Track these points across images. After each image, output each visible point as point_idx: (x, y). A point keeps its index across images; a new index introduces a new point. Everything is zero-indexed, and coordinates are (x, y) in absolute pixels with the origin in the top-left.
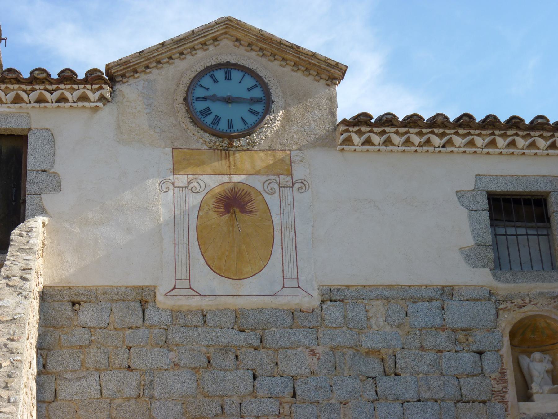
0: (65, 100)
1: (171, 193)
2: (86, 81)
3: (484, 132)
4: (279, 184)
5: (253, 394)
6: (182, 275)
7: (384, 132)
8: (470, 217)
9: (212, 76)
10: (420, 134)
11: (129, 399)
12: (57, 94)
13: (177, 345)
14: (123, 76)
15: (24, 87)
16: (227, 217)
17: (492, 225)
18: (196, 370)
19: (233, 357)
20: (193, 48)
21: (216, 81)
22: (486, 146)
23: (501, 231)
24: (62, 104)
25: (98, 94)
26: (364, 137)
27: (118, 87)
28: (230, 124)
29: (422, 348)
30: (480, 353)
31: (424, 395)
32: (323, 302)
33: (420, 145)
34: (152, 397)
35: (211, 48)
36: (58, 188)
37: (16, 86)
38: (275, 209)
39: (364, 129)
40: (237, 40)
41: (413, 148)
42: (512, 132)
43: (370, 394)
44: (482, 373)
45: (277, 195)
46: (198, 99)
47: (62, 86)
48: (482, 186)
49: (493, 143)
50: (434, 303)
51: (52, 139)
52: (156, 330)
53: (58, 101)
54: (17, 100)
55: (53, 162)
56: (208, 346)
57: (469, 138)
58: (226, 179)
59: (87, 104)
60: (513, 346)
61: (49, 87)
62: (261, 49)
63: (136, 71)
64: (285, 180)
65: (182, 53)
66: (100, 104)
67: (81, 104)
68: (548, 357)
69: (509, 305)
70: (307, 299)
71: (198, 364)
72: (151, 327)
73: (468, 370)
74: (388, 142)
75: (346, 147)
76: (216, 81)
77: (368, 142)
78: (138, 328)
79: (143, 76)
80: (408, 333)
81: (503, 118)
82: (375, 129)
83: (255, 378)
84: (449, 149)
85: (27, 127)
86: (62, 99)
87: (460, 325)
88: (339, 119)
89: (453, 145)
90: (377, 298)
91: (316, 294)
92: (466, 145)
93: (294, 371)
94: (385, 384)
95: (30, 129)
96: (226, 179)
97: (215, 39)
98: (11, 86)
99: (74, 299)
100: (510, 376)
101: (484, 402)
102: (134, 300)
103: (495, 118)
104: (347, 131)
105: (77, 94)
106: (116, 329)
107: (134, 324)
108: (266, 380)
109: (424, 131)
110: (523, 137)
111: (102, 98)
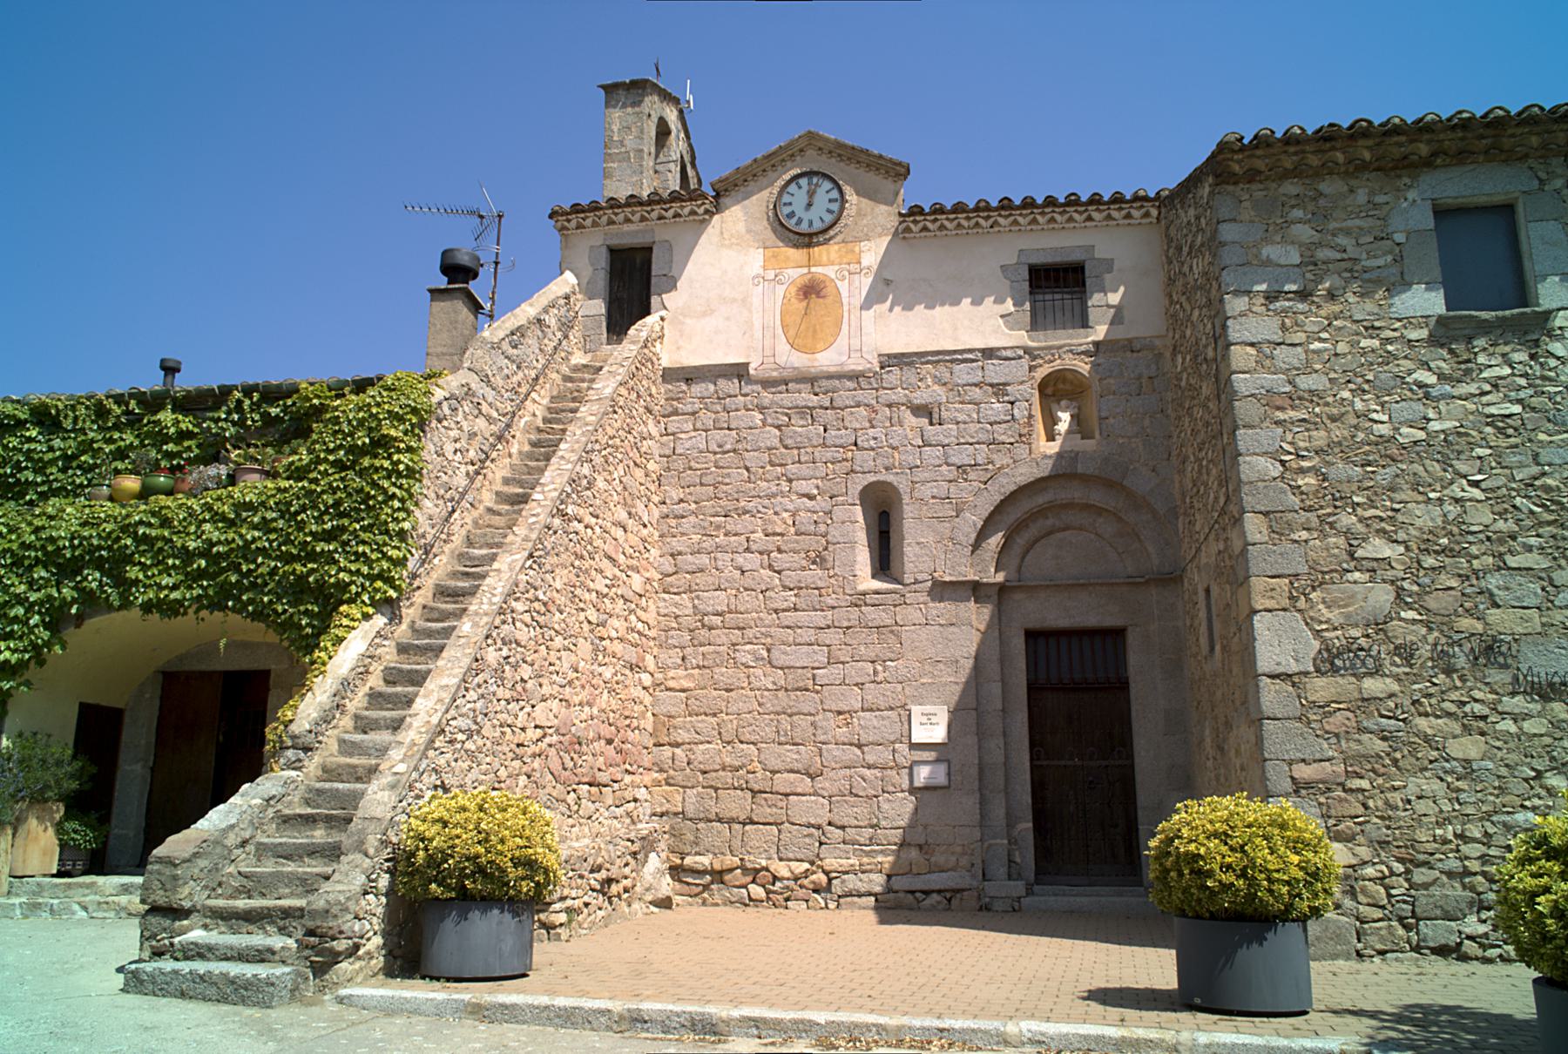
0: (680, 216)
3: (1024, 212)
6: (768, 352)
7: (936, 220)
8: (1011, 287)
10: (968, 219)
11: (728, 452)
12: (671, 212)
14: (726, 190)
16: (804, 304)
17: (1031, 293)
18: (778, 427)
20: (783, 160)
22: (1029, 224)
23: (1040, 297)
27: (722, 200)
28: (811, 223)
30: (1012, 403)
31: (962, 441)
33: (969, 228)
35: (798, 158)
38: (845, 294)
39: (918, 218)
40: (820, 149)
42: (1050, 210)
46: (785, 204)
48: (1023, 259)
49: (1034, 221)
51: (671, 249)
53: (674, 217)
54: (643, 219)
55: (671, 267)
57: (1012, 218)
58: (805, 270)
59: (696, 218)
62: (840, 155)
63: (736, 185)
64: (853, 267)
65: (773, 166)
66: (707, 217)
67: (691, 218)
68: (1074, 404)
69: (1041, 361)
74: (943, 227)
77: (925, 229)
79: (742, 189)
84: (996, 229)
86: (677, 215)
89: (1000, 225)
92: (1011, 225)
96: (805, 270)
97: (801, 150)
105: (686, 211)
106: (719, 398)
107: (732, 393)
108: (833, 433)
110: (1060, 213)
111: (707, 212)
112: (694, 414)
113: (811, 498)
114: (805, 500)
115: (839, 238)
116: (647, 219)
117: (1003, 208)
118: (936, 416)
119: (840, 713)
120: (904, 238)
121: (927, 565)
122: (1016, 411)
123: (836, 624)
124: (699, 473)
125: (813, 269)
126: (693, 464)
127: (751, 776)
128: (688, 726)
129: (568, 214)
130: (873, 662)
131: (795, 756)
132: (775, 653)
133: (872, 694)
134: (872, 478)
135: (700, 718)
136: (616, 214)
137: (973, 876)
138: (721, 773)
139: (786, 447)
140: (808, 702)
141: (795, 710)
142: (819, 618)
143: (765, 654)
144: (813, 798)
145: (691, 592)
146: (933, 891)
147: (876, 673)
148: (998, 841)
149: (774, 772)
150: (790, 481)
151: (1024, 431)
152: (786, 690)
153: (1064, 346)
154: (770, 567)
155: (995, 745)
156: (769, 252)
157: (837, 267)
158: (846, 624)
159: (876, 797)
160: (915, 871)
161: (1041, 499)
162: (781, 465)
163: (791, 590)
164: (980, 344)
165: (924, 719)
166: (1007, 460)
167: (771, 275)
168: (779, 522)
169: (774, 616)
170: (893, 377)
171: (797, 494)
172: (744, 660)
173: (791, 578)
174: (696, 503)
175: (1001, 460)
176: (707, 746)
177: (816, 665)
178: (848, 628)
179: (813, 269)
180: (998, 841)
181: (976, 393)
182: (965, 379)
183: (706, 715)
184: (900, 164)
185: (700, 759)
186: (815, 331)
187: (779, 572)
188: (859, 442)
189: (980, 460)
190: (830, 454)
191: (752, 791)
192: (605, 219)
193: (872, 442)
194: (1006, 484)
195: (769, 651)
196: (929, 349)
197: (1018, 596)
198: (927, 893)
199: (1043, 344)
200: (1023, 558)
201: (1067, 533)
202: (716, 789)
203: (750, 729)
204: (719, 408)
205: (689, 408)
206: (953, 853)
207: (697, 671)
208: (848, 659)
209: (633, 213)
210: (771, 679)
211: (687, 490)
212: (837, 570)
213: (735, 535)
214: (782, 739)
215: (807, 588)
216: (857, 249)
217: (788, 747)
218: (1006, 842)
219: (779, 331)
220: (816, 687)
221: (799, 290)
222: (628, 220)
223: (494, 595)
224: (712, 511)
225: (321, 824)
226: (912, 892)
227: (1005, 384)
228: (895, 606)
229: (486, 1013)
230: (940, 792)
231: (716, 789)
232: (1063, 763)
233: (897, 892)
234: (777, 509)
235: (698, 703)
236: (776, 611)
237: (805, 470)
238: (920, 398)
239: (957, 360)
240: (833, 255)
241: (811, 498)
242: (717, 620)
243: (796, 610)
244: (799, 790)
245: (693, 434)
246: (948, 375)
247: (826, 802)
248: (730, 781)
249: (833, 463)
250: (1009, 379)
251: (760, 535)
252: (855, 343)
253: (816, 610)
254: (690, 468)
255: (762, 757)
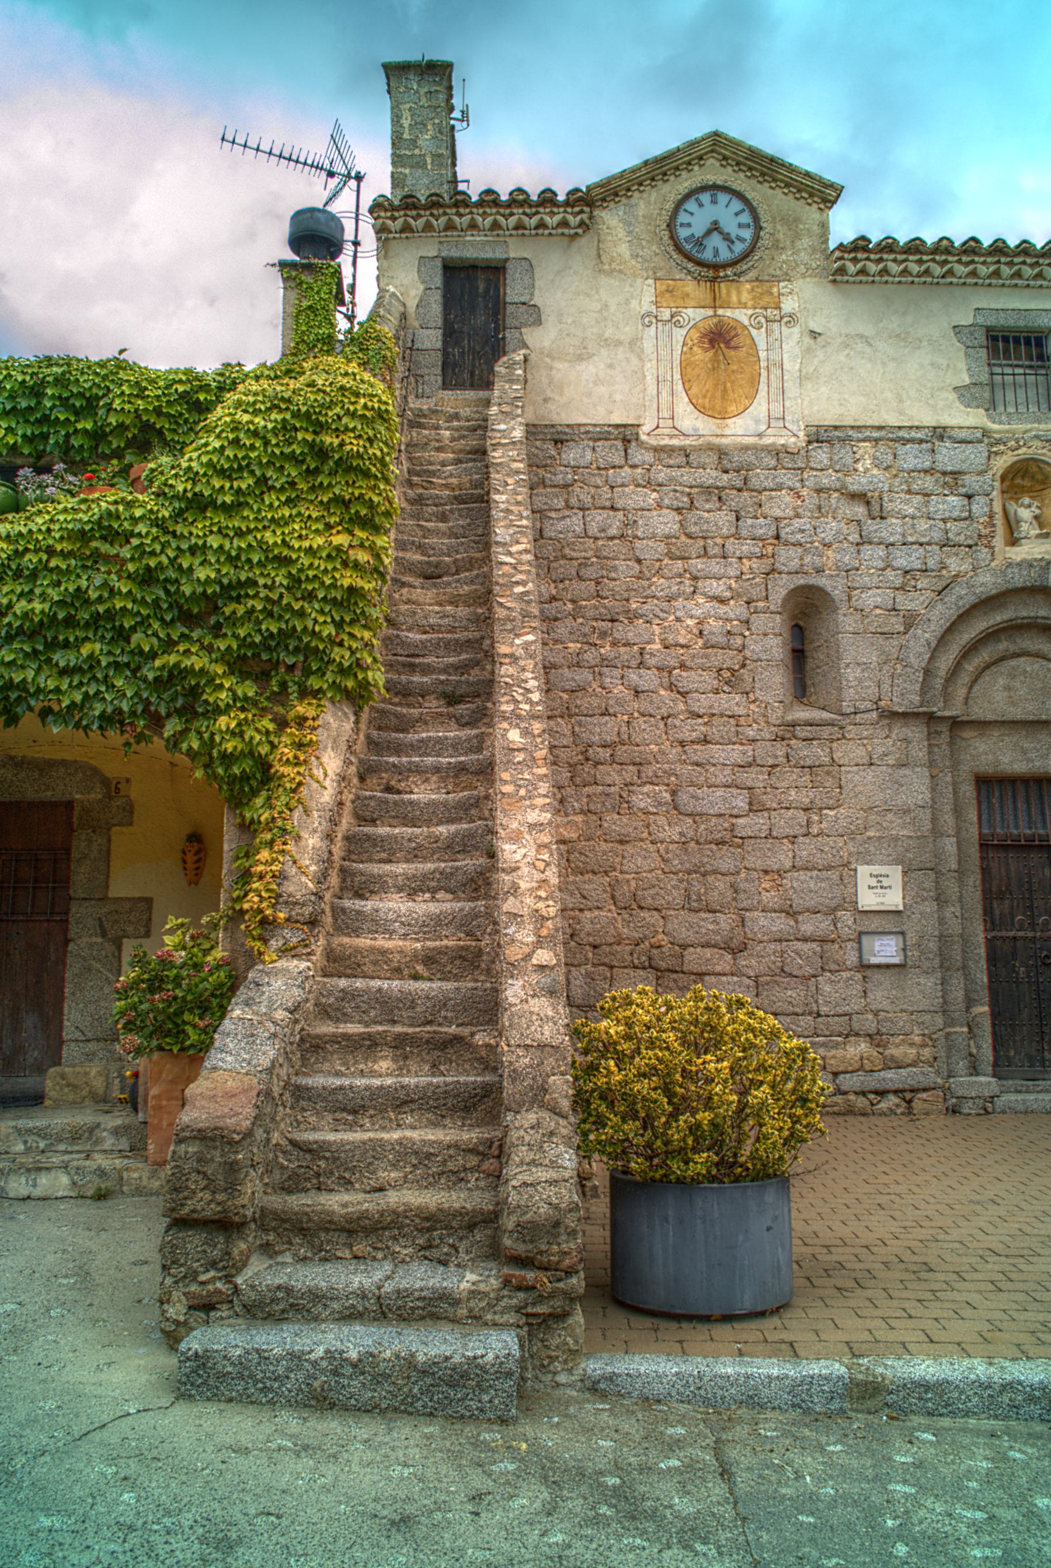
1: (653, 328)
2: (567, 203)
3: (989, 260)
4: (766, 317)
5: (737, 536)
7: (881, 260)
8: (966, 354)
9: (697, 200)
10: (920, 262)
11: (612, 538)
13: (660, 485)
14: (604, 200)
15: (502, 211)
16: (710, 354)
18: (678, 510)
19: (716, 499)
21: (701, 205)
24: (540, 231)
25: (578, 218)
26: (859, 266)
29: (909, 492)
30: (969, 497)
31: (910, 539)
32: (809, 442)
33: (918, 276)
34: (636, 537)
36: (538, 322)
37: (494, 210)
38: (762, 345)
39: (860, 256)
41: (910, 279)
43: (854, 537)
44: (970, 518)
45: (763, 330)
46: (682, 225)
47: (541, 210)
48: (980, 320)
50: (924, 446)
52: (639, 470)
53: (537, 228)
55: (532, 294)
56: (691, 487)
57: (971, 267)
59: (566, 231)
60: (1003, 492)
61: (528, 211)
63: (616, 195)
69: (1002, 447)
70: (793, 439)
71: (681, 505)
72: (634, 466)
73: (955, 514)
75: (839, 278)
76: (701, 205)
77: (863, 272)
78: (621, 467)
79: (624, 200)
80: (896, 476)
81: (1012, 242)
82: (872, 256)
83: (738, 520)
85: (505, 256)
87: (949, 469)
88: (832, 245)
90: (864, 440)
91: (801, 434)
92: (968, 275)
93: (779, 513)
94: (871, 526)
95: (507, 260)
97: (701, 158)
98: (488, 210)
99: (557, 437)
100: (999, 520)
101: (970, 547)
102: (616, 439)
103: (1004, 242)
104: (841, 258)
105: (557, 218)
106: (599, 468)
108: (749, 521)
109: (925, 258)
111: (582, 224)
112: (566, 486)
113: (722, 601)
114: (714, 604)
115: (752, 275)
116: (500, 227)
117: (965, 252)
118: (876, 507)
119: (766, 872)
120: (834, 281)
121: (873, 691)
122: (974, 507)
123: (759, 761)
124: (575, 563)
125: (720, 312)
126: (567, 551)
127: (655, 951)
128: (571, 887)
129: (394, 208)
130: (805, 810)
131: (711, 927)
132: (683, 797)
133: (806, 849)
134: (801, 581)
135: (586, 877)
136: (461, 215)
137: (938, 1073)
138: (616, 947)
139: (689, 536)
140: (726, 861)
141: (708, 868)
142: (736, 753)
143: (667, 796)
144: (735, 979)
145: (570, 716)
146: (888, 1092)
147: (809, 823)
148: (958, 1029)
149: (684, 947)
150: (695, 578)
151: (984, 532)
152: (698, 843)
153: (1030, 430)
154: (671, 687)
155: (952, 910)
156: (662, 286)
157: (750, 312)
158: (771, 762)
159: (815, 976)
160: (868, 1065)
161: (999, 617)
162: (683, 558)
163: (699, 716)
164: (928, 419)
165: (873, 882)
166: (965, 567)
167: (666, 314)
168: (683, 632)
169: (679, 749)
170: (821, 455)
171: (704, 594)
172: (642, 805)
173: (702, 703)
174: (573, 601)
175: (955, 565)
176: (597, 913)
177: (735, 812)
178: (773, 766)
179: (720, 312)
180: (958, 1029)
181: (928, 483)
182: (911, 463)
183: (594, 873)
184: (831, 186)
185: (588, 927)
186: (725, 391)
187: (684, 694)
188: (783, 534)
189: (931, 563)
190: (747, 547)
191: (657, 970)
192: (443, 220)
193: (799, 536)
194: (962, 596)
195: (674, 793)
196: (870, 423)
197: (967, 734)
198: (881, 1093)
199: (1007, 427)
200: (971, 688)
201: (1022, 659)
202: (612, 967)
203: (652, 892)
204: (599, 482)
205: (559, 479)
206: (912, 1045)
207: (579, 818)
208: (774, 805)
209: (484, 215)
210: (678, 829)
211: (561, 586)
212: (758, 694)
213: (624, 645)
214: (695, 904)
215: (722, 715)
216: (775, 290)
217: (703, 915)
218: (965, 1029)
219: (679, 387)
220: (730, 840)
221: (704, 336)
222: (473, 226)
223: (528, 691)
224: (591, 613)
225: (387, 1052)
226: (863, 1093)
227: (960, 473)
228: (832, 741)
229: (889, 1399)
230: (893, 971)
231: (612, 967)
232: (1012, 934)
233: (845, 1093)
234: (678, 614)
235: (583, 858)
236: (682, 744)
237: (715, 566)
238: (854, 484)
239: (903, 439)
240: (745, 297)
241: (722, 601)
242: (604, 754)
243: (705, 741)
244: (718, 969)
245: (567, 513)
246: (890, 457)
247: (752, 983)
248: (628, 958)
249: (750, 559)
250: (964, 467)
251: (657, 646)
252: (777, 410)
253: (734, 744)
254: (564, 557)
255: (670, 926)
